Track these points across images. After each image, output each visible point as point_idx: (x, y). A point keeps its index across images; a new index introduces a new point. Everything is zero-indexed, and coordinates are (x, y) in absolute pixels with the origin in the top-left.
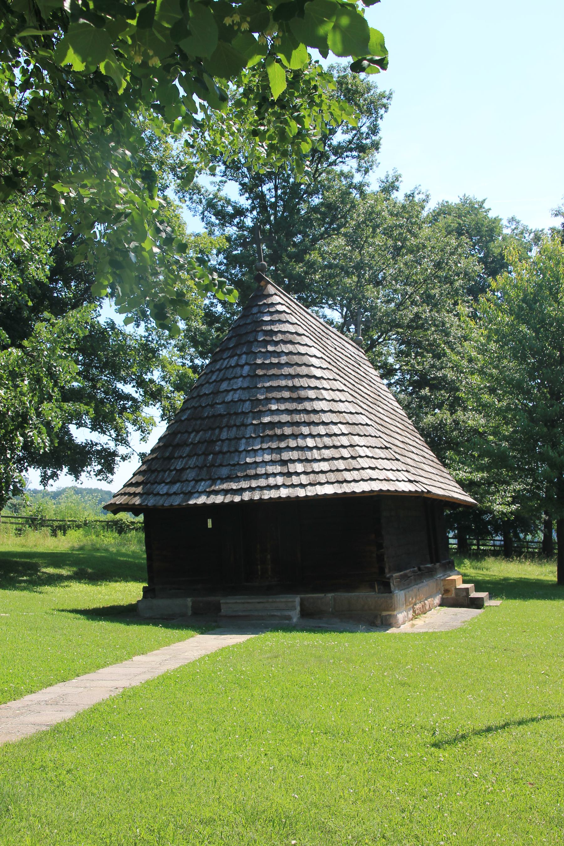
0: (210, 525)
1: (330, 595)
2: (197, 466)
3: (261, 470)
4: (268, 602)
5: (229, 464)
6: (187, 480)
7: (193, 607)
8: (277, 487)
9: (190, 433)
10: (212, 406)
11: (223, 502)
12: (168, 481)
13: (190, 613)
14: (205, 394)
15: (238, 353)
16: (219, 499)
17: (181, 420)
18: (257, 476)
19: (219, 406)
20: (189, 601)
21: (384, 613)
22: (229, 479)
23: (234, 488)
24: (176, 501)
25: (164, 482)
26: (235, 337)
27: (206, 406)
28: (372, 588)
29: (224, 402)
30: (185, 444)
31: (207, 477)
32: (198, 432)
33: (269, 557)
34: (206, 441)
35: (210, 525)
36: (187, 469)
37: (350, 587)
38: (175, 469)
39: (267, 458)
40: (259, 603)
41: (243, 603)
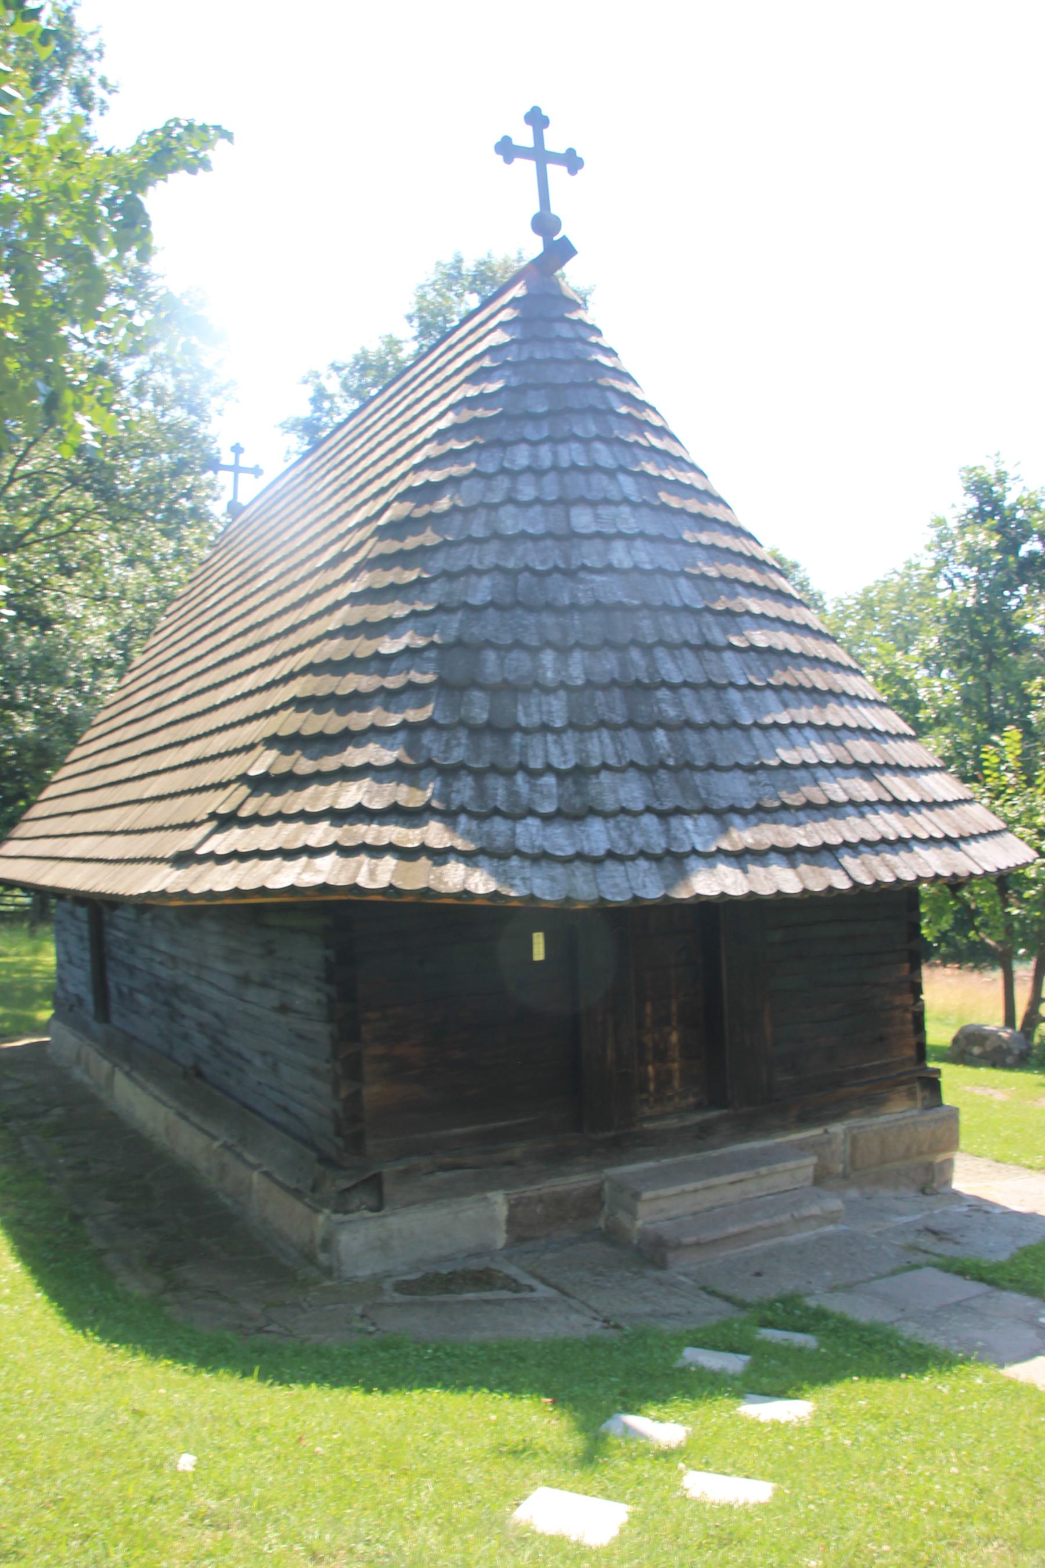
0: (539, 952)
1: (837, 1129)
2: (632, 764)
3: (836, 790)
4: (759, 1176)
5: (738, 766)
6: (624, 811)
7: (511, 1221)
8: (902, 844)
9: (534, 651)
10: (569, 574)
11: (805, 891)
12: (548, 807)
13: (501, 1239)
14: (524, 535)
15: (578, 431)
16: (783, 880)
17: (466, 606)
18: (832, 809)
19: (598, 578)
20: (499, 1203)
21: (940, 1158)
22: (760, 813)
23: (805, 843)
24: (649, 885)
25: (532, 813)
26: (536, 387)
27: (548, 573)
28: (911, 1095)
29: (609, 569)
30: (537, 684)
31: (695, 805)
32: (563, 651)
33: (674, 1038)
34: (614, 683)
35: (539, 952)
36: (596, 771)
37: (872, 1102)
38: (549, 768)
39: (825, 752)
40: (733, 1183)
41: (696, 1191)
